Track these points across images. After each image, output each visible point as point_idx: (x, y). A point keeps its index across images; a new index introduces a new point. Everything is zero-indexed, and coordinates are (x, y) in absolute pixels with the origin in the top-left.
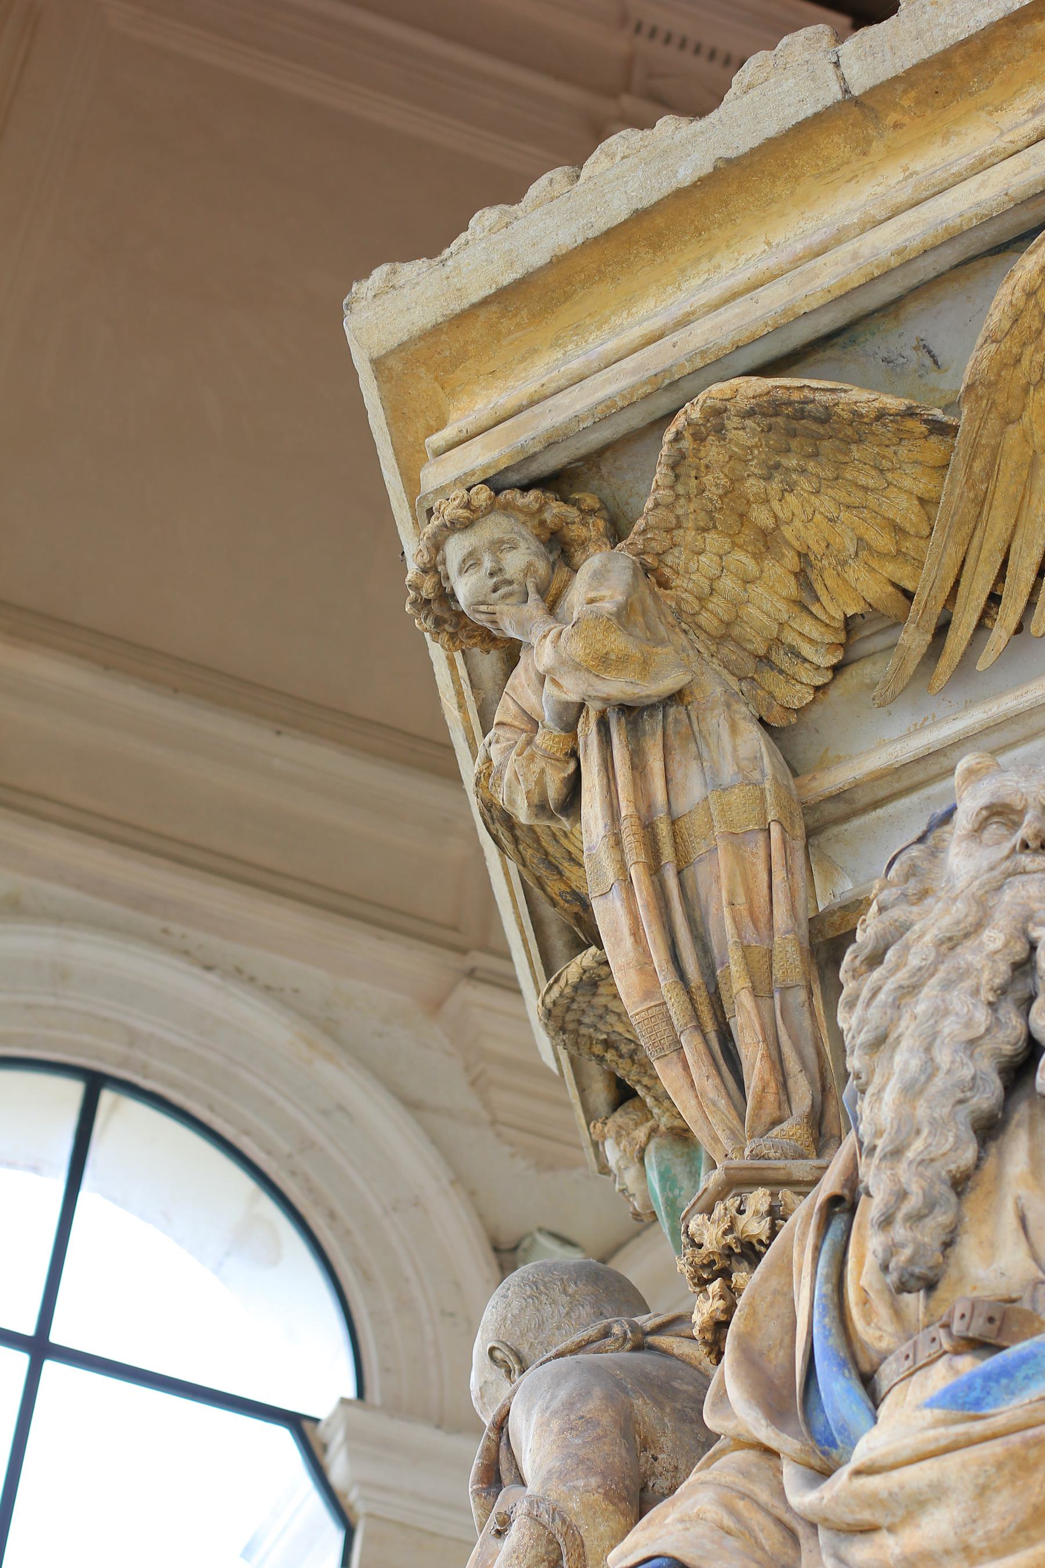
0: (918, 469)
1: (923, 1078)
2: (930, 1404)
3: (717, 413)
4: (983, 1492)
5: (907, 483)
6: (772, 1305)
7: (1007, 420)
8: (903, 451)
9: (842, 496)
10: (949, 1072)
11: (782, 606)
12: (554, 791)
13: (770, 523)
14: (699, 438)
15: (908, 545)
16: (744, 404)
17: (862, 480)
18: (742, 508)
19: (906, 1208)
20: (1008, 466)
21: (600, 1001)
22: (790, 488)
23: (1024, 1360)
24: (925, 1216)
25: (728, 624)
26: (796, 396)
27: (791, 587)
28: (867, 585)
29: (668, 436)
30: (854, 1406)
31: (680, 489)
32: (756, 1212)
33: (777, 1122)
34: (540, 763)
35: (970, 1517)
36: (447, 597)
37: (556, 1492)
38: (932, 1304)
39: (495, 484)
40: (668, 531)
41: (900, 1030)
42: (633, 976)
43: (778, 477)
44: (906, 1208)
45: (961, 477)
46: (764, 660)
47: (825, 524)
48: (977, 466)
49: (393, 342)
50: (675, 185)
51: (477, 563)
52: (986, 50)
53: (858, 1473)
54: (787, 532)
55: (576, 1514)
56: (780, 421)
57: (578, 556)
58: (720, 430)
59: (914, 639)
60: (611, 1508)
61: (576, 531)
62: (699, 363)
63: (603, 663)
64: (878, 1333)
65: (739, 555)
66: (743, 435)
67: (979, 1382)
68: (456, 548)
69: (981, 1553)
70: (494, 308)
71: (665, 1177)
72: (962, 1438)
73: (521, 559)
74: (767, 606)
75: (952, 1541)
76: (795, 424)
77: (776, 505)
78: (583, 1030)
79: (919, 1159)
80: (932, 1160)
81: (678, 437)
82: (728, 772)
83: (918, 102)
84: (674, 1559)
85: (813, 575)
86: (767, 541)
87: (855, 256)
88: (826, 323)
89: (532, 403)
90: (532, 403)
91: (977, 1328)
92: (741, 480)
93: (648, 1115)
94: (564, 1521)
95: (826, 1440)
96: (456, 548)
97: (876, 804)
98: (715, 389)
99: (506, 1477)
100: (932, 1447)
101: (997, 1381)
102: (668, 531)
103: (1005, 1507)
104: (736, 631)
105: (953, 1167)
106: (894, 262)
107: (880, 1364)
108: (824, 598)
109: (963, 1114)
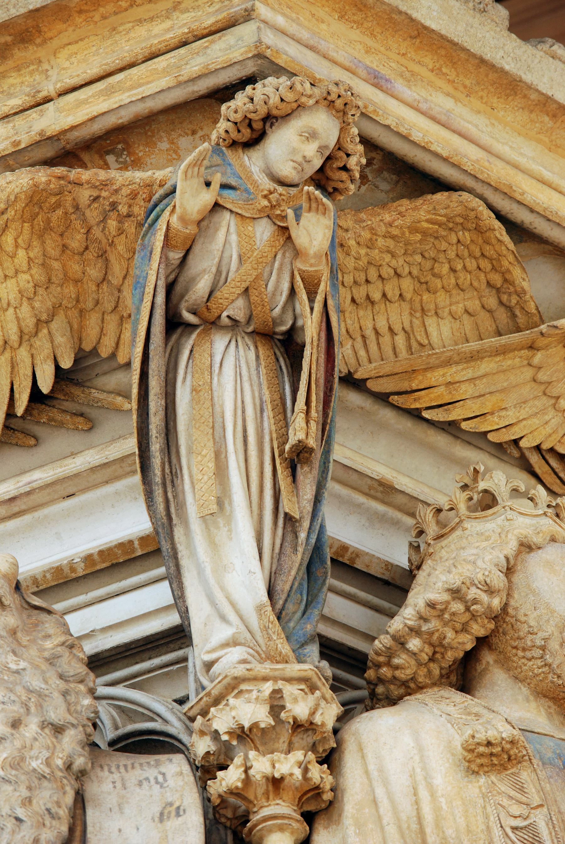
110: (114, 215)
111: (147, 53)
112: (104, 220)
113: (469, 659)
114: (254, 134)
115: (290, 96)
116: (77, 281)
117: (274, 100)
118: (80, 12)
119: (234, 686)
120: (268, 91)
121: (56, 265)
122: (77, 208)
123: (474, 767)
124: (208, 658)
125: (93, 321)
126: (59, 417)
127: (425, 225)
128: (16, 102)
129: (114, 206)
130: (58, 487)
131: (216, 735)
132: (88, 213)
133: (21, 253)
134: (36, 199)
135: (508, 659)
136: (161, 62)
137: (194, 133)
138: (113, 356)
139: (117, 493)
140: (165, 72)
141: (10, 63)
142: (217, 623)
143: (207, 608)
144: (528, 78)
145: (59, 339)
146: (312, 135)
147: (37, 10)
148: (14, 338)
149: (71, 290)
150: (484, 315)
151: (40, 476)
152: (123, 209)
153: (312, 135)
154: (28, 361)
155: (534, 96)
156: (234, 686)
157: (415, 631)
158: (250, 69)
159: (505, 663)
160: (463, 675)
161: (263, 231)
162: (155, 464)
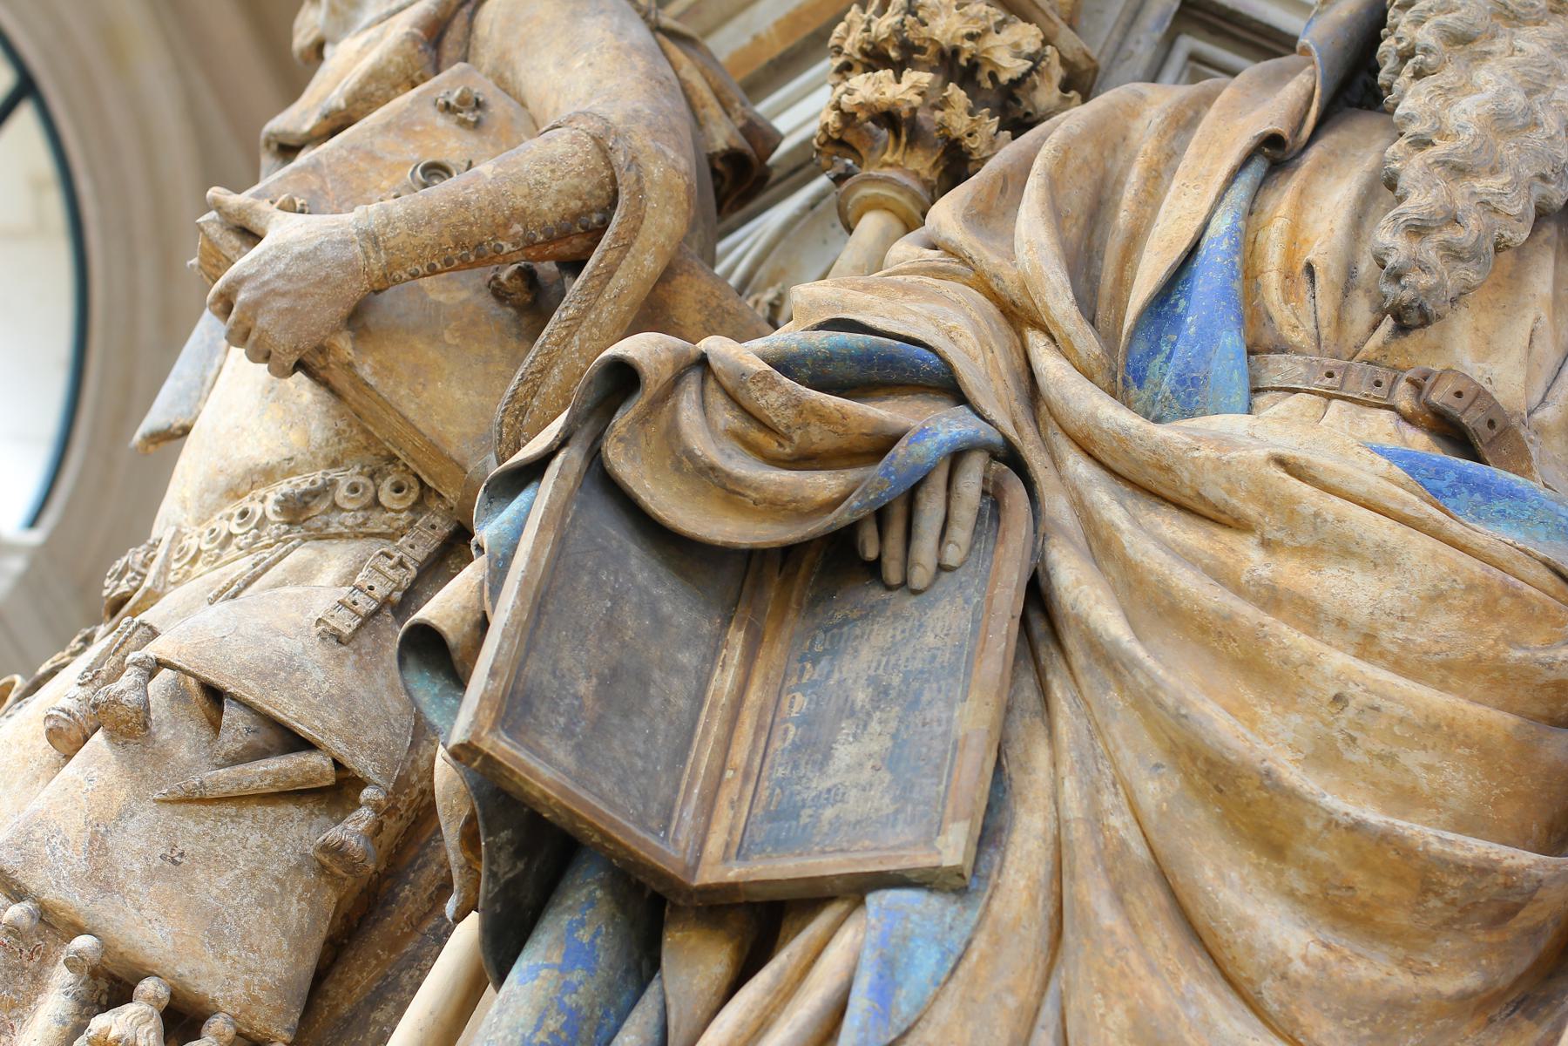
1: (1520, 121)
4: (1436, 598)
6: (1079, 170)
10: (1550, 138)
23: (1512, 494)
24: (1462, 260)
30: (1236, 375)
32: (1016, 45)
35: (1403, 611)
37: (640, 139)
38: (1393, 346)
41: (1493, 48)
53: (1281, 462)
55: (652, 182)
60: (685, 206)
64: (1293, 321)
67: (1451, 476)
69: (1382, 655)
72: (1431, 523)
75: (1361, 616)
79: (1484, 197)
80: (1496, 211)
84: (948, 366)
91: (1471, 419)
94: (639, 180)
95: (1135, 371)
100: (1393, 505)
101: (1471, 492)
103: (1443, 629)
105: (1508, 234)
107: (1269, 351)
109: (1538, 190)
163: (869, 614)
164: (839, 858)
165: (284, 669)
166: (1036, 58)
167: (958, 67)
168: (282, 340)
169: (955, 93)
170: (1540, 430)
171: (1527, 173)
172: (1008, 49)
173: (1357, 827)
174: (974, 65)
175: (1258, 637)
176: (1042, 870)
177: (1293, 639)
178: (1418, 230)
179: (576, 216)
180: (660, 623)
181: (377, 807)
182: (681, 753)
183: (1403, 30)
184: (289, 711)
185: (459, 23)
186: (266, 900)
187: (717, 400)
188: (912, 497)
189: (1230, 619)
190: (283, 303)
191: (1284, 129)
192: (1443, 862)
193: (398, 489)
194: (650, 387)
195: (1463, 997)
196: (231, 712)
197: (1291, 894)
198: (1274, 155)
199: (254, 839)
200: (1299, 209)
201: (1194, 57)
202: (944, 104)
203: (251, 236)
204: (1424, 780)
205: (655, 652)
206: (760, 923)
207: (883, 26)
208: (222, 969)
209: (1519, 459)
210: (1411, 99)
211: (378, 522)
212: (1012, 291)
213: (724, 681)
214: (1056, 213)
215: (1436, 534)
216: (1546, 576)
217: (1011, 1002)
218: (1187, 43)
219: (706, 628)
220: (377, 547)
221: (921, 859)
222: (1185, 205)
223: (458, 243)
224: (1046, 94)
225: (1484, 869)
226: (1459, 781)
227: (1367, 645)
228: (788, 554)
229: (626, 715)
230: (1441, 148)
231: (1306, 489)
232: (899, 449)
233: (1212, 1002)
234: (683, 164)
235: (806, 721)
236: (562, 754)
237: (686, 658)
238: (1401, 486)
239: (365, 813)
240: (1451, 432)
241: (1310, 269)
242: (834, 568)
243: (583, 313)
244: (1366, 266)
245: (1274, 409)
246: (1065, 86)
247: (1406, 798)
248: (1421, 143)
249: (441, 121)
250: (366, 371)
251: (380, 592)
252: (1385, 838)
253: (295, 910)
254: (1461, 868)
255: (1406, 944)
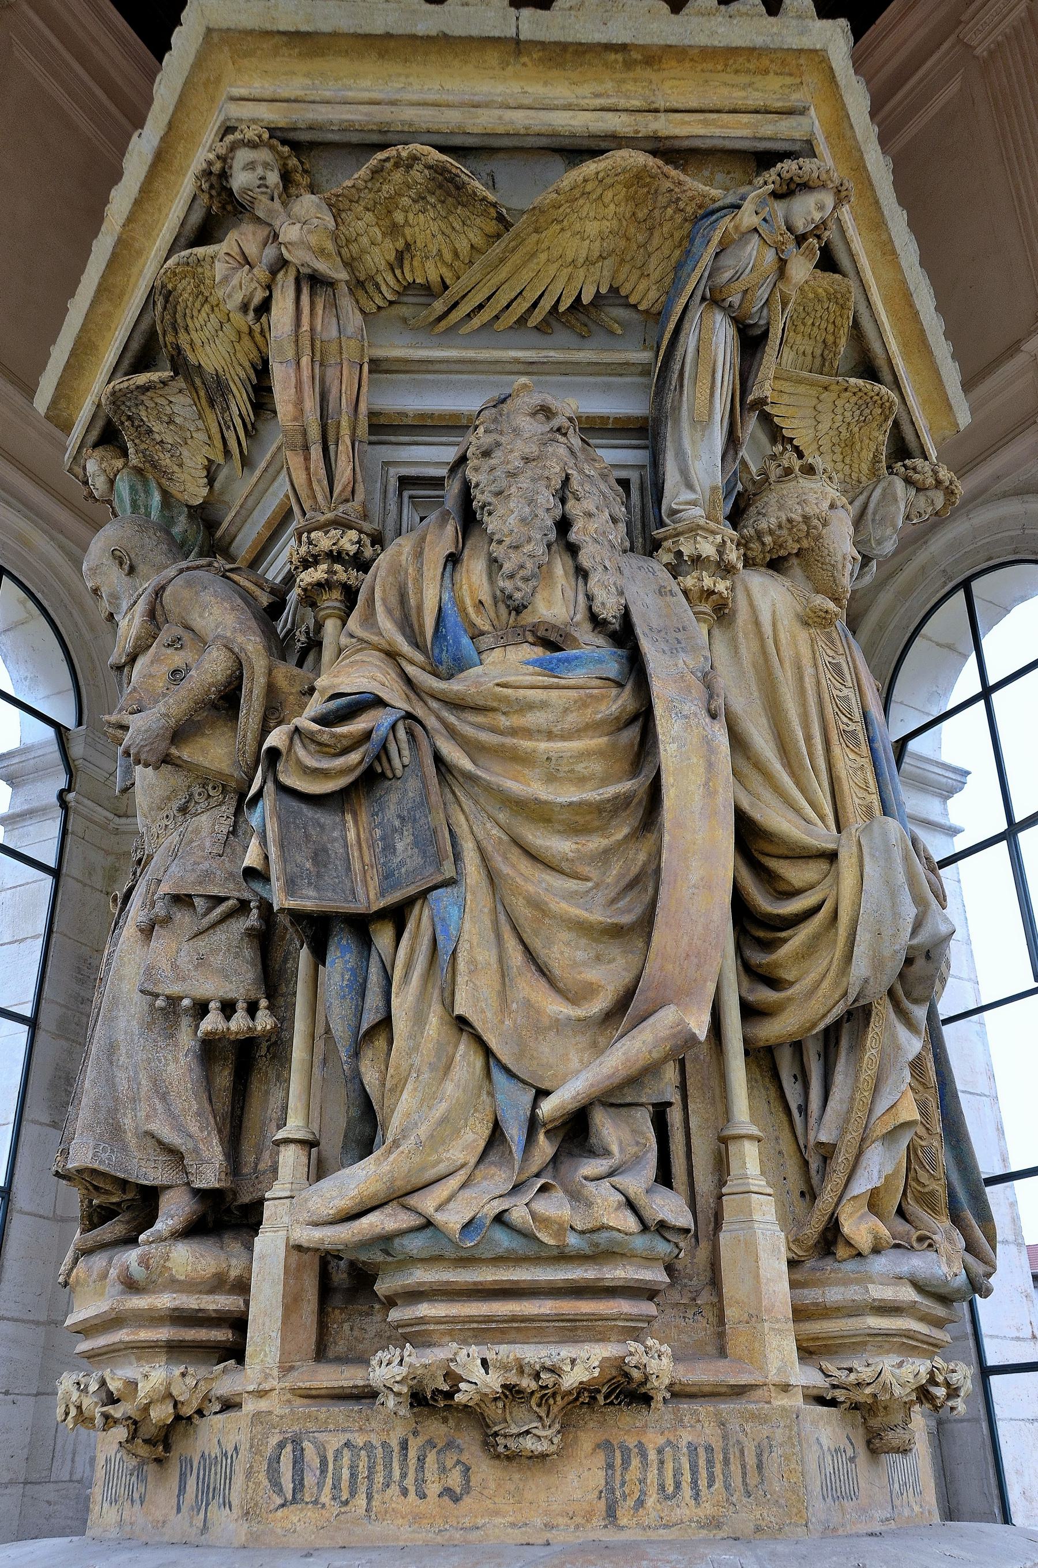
0: (479, 232)
2: (528, 663)
3: (414, 158)
5: (471, 235)
7: (537, 231)
8: (478, 220)
9: (443, 226)
11: (383, 262)
12: (257, 300)
13: (402, 222)
14: (397, 165)
15: (456, 263)
16: (431, 162)
17: (455, 224)
18: (391, 208)
19: (522, 573)
20: (522, 251)
21: (144, 398)
22: (424, 211)
25: (353, 259)
26: (454, 170)
27: (392, 257)
28: (432, 273)
29: (381, 155)
31: (369, 185)
33: (347, 501)
34: (255, 284)
36: (224, 175)
39: (273, 131)
40: (351, 201)
42: (290, 407)
43: (421, 203)
44: (522, 573)
45: (503, 245)
46: (361, 284)
47: (429, 236)
48: (513, 244)
49: (224, 25)
50: (414, 31)
51: (253, 169)
52: (584, 53)
53: (498, 685)
54: (408, 231)
56: (440, 178)
57: (293, 190)
58: (410, 167)
59: (439, 306)
61: (298, 177)
62: (406, 129)
63: (322, 252)
65: (376, 229)
66: (418, 174)
68: (243, 156)
70: (285, 39)
71: (133, 489)
73: (273, 178)
74: (376, 260)
75: (544, 727)
76: (445, 183)
77: (411, 216)
78: (123, 407)
81: (387, 159)
82: (350, 330)
83: (540, 59)
85: (407, 256)
86: (394, 231)
87: (500, 118)
88: (470, 142)
89: (296, 101)
90: (296, 101)
92: (401, 195)
93: (125, 453)
96: (243, 156)
97: (387, 372)
98: (419, 146)
99: (160, 619)
102: (351, 201)
103: (573, 719)
104: (356, 264)
106: (522, 131)
108: (407, 270)
110: (673, 206)
111: (732, 107)
112: (666, 208)
113: (784, 559)
114: (788, 190)
115: (824, 177)
116: (628, 239)
117: (815, 175)
118: (692, 60)
119: (694, 530)
120: (808, 165)
121: (625, 223)
122: (656, 191)
123: (810, 621)
124: (674, 506)
125: (626, 269)
126: (573, 322)
127: (820, 290)
128: (636, 103)
129: (678, 199)
130: (562, 366)
131: (679, 554)
132: (660, 198)
133: (612, 206)
134: (639, 177)
135: (808, 565)
136: (745, 118)
137: (729, 173)
138: (627, 297)
139: (595, 384)
140: (746, 126)
141: (631, 75)
142: (683, 489)
143: (678, 477)
144: (890, 224)
145: (605, 272)
146: (821, 208)
147: (670, 46)
148: (581, 260)
149: (623, 243)
150: (810, 357)
151: (554, 355)
152: (682, 205)
153: (821, 208)
154: (582, 279)
155: (884, 237)
156: (694, 530)
157: (771, 532)
158: (797, 147)
159: (806, 567)
160: (776, 565)
161: (770, 256)
162: (663, 377)
163: (388, 791)
164: (413, 886)
165: (207, 876)
166: (359, 542)
167: (335, 557)
168: (152, 759)
169: (338, 567)
170: (577, 624)
171: (539, 537)
172: (348, 541)
173: (571, 804)
174: (339, 553)
175: (514, 748)
176: (478, 860)
177: (527, 744)
178: (511, 576)
179: (231, 676)
180: (322, 827)
181: (258, 908)
182: (349, 869)
183: (480, 497)
184: (215, 891)
185: (158, 607)
186: (237, 956)
187: (307, 741)
188: (384, 748)
189: (503, 745)
190: (147, 748)
191: (453, 550)
192: (602, 802)
193: (214, 788)
194: (284, 751)
195: (626, 837)
196: (197, 901)
197: (559, 831)
198: (453, 560)
199: (224, 937)
200: (469, 578)
201: (411, 497)
202: (335, 573)
203: (125, 728)
204: (586, 772)
205: (325, 838)
206: (397, 916)
207: (303, 550)
208: (233, 987)
209: (574, 643)
210: (492, 524)
211: (213, 802)
212: (386, 647)
213: (351, 835)
214: (389, 611)
215: (558, 687)
216: (598, 682)
217: (486, 910)
218: (406, 494)
219: (338, 819)
220: (215, 811)
221: (440, 879)
222: (430, 597)
223: (196, 703)
224: (368, 552)
225: (616, 797)
226: (597, 767)
227: (550, 736)
228: (354, 784)
229: (325, 866)
230: (508, 541)
231: (510, 691)
232: (374, 735)
233: (548, 878)
234: (258, 639)
235: (383, 838)
236: (312, 893)
237: (335, 834)
238: (539, 675)
239: (255, 911)
240: (552, 646)
241: (480, 602)
242: (370, 780)
243: (249, 710)
244: (498, 593)
245: (490, 658)
246: (373, 546)
247: (581, 780)
248: (500, 542)
249: (169, 651)
250: (185, 757)
251: (225, 831)
252: (580, 804)
253: (248, 953)
254: (608, 801)
255: (602, 830)
